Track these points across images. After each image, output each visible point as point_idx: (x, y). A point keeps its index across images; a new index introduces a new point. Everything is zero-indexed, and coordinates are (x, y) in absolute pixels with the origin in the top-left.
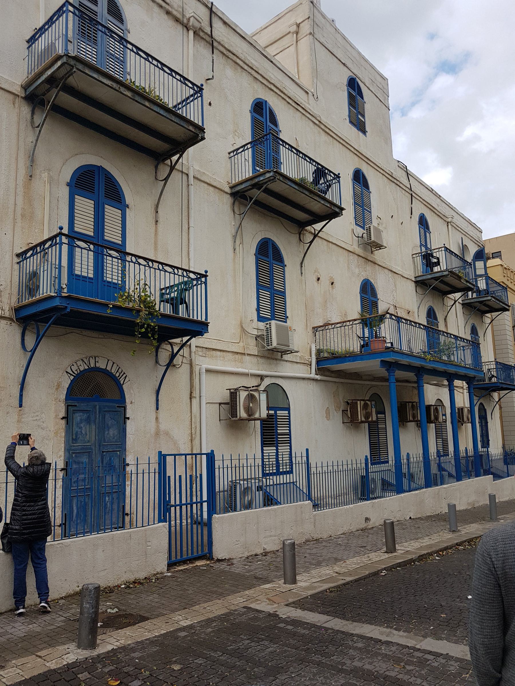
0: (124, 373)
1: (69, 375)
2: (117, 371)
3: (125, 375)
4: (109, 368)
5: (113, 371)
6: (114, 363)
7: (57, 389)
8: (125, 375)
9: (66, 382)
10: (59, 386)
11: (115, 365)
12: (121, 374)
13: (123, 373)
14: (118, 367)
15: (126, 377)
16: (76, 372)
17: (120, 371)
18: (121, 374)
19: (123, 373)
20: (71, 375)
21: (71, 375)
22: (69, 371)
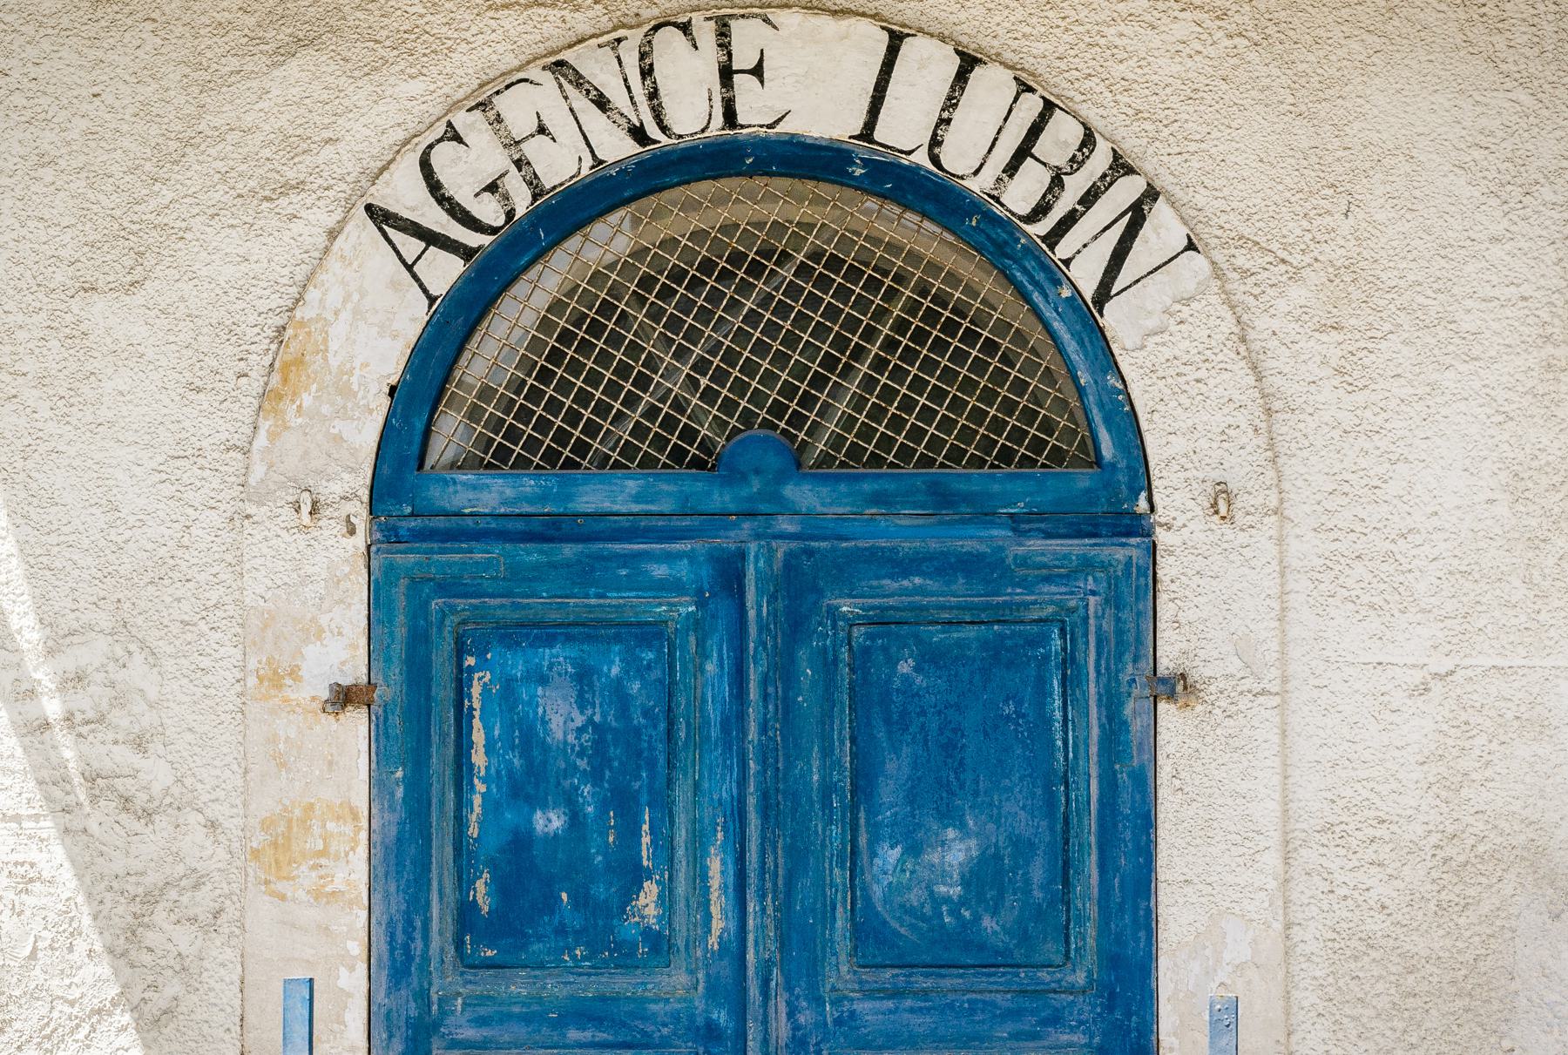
0: (1121, 166)
1: (411, 246)
2: (1023, 152)
3: (1126, 191)
4: (904, 130)
5: (959, 157)
6: (968, 63)
7: (269, 399)
8: (1126, 191)
9: (375, 319)
10: (286, 363)
11: (990, 86)
12: (1075, 186)
13: (1100, 161)
14: (1030, 107)
15: (1137, 215)
16: (489, 211)
17: (1060, 138)
18: (1075, 186)
19: (1100, 161)
20: (431, 238)
21: (431, 238)
22: (405, 194)
